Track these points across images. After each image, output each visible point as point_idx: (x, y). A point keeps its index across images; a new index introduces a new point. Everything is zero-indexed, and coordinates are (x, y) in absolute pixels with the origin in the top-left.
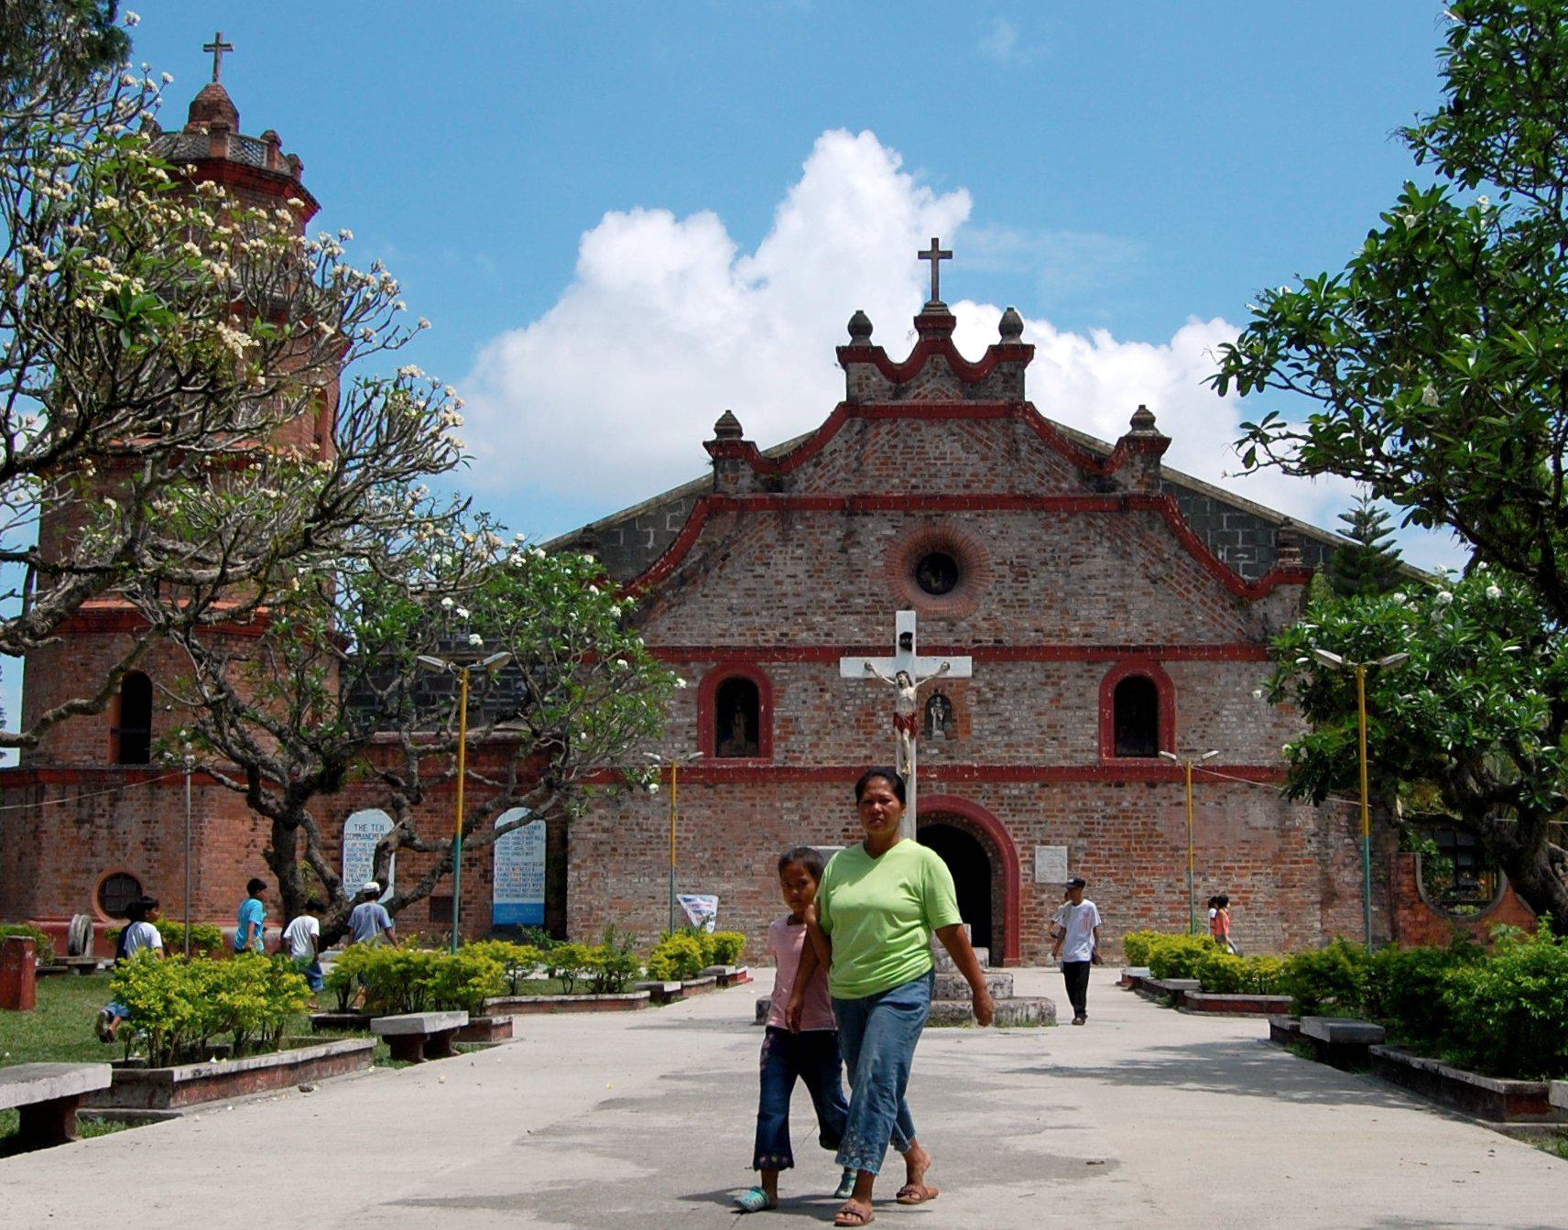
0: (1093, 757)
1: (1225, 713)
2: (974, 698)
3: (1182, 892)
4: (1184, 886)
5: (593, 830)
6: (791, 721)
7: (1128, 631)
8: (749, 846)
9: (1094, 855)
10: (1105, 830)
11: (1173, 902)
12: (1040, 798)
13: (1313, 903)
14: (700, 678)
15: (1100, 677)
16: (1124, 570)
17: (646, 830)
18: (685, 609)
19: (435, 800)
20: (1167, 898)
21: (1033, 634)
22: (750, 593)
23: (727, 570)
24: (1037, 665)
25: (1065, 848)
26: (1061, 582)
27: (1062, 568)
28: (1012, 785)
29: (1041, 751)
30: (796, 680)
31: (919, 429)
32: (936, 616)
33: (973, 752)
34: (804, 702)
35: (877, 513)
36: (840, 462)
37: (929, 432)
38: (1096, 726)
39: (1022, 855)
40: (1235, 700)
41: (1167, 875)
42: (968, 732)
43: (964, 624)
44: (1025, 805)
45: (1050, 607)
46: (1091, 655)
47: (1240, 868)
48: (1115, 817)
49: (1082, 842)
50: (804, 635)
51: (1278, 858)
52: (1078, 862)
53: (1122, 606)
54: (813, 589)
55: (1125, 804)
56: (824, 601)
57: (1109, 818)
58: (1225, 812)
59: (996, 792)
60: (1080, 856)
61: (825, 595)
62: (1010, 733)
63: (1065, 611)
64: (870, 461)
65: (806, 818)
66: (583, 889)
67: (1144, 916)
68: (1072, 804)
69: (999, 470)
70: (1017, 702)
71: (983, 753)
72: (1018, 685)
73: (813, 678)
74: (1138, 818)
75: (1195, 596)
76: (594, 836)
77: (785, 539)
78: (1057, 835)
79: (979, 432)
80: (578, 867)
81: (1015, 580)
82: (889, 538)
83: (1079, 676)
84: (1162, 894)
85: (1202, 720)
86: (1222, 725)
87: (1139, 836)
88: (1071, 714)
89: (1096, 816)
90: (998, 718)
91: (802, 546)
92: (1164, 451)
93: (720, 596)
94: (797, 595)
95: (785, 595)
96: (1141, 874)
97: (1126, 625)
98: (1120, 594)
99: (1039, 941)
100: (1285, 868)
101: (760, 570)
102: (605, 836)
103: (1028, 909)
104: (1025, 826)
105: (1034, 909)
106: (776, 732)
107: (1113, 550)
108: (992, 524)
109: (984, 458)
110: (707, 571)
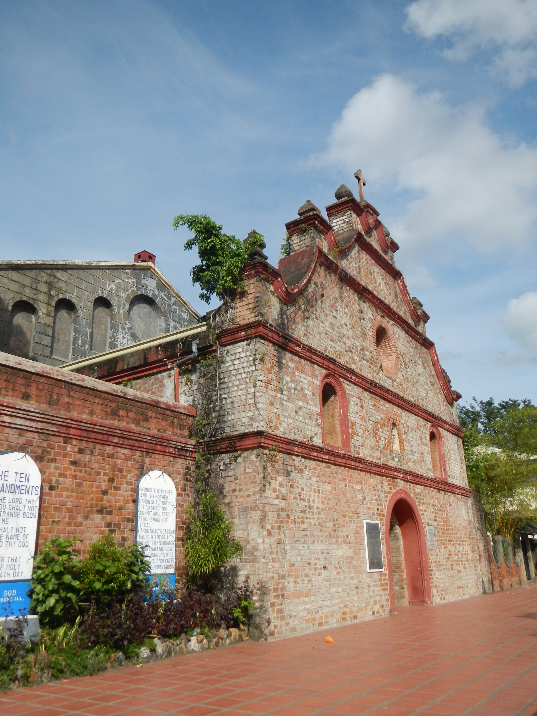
5: (277, 497)
14: (319, 378)
17: (303, 500)
18: (310, 323)
19: (81, 451)
23: (324, 306)
28: (417, 486)
32: (389, 375)
34: (357, 412)
40: (452, 452)
48: (439, 510)
49: (435, 524)
55: (441, 503)
61: (358, 344)
66: (274, 556)
67: (452, 569)
76: (276, 502)
82: (372, 320)
92: (427, 322)
95: (344, 335)
100: (472, 540)
101: (335, 313)
110: (316, 300)
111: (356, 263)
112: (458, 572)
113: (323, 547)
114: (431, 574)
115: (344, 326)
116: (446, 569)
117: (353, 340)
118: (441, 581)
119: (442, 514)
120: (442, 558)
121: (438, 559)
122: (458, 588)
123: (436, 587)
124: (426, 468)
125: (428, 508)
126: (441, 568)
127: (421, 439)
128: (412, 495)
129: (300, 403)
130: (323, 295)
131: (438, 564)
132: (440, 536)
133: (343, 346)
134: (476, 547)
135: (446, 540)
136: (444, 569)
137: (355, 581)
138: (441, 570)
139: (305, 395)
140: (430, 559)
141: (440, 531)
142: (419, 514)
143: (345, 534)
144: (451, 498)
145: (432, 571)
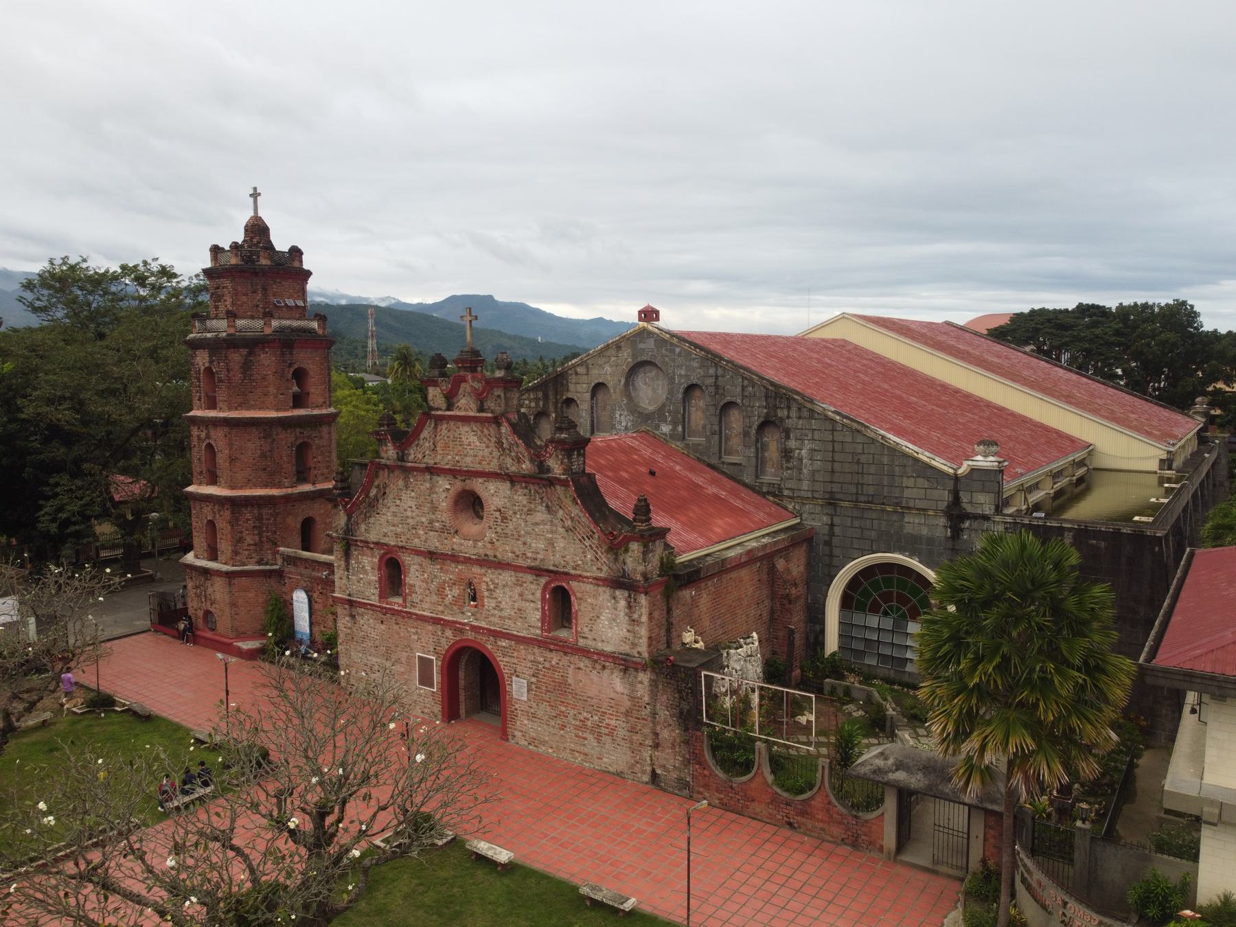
1: (603, 618)
2: (485, 587)
3: (580, 721)
4: (581, 717)
5: (345, 627)
6: (412, 586)
7: (552, 560)
8: (399, 649)
9: (539, 688)
10: (544, 676)
11: (576, 726)
12: (514, 650)
13: (647, 746)
16: (552, 522)
18: (372, 520)
21: (510, 555)
22: (394, 514)
23: (386, 501)
24: (513, 573)
25: (525, 681)
26: (523, 525)
27: (524, 517)
29: (515, 623)
30: (414, 564)
31: (458, 428)
33: (486, 618)
35: (442, 476)
36: (427, 444)
37: (464, 429)
40: (608, 611)
41: (574, 709)
42: (483, 606)
43: (480, 544)
45: (518, 540)
46: (538, 571)
47: (610, 714)
48: (549, 669)
49: (533, 680)
50: (416, 540)
51: (628, 714)
52: (532, 690)
53: (551, 543)
54: (418, 516)
55: (553, 663)
56: (423, 523)
57: (547, 668)
58: (601, 678)
59: (496, 642)
60: (533, 686)
61: (424, 520)
62: (501, 610)
63: (525, 544)
64: (439, 445)
65: (420, 639)
67: (563, 730)
69: (494, 453)
70: (504, 593)
71: (490, 619)
72: (504, 583)
73: (420, 565)
74: (559, 672)
75: (587, 543)
77: (407, 487)
78: (523, 673)
79: (486, 431)
80: (341, 644)
81: (502, 520)
83: (532, 583)
84: (571, 719)
85: (591, 620)
87: (560, 683)
88: (528, 604)
89: (540, 666)
90: (494, 601)
91: (413, 491)
93: (383, 514)
94: (413, 518)
95: (408, 517)
97: (553, 556)
98: (550, 536)
99: (516, 729)
101: (398, 502)
102: (349, 631)
103: (511, 711)
106: (407, 591)
107: (547, 506)
108: (492, 486)
109: (488, 447)
111: (429, 442)
112: (577, 736)
113: (378, 660)
115: (409, 509)
117: (418, 518)
119: (554, 674)
121: (532, 711)
122: (574, 751)
126: (534, 719)
127: (521, 595)
128: (489, 647)
129: (362, 576)
130: (385, 493)
133: (406, 526)
134: (647, 731)
139: (366, 570)
142: (499, 666)
144: (584, 663)
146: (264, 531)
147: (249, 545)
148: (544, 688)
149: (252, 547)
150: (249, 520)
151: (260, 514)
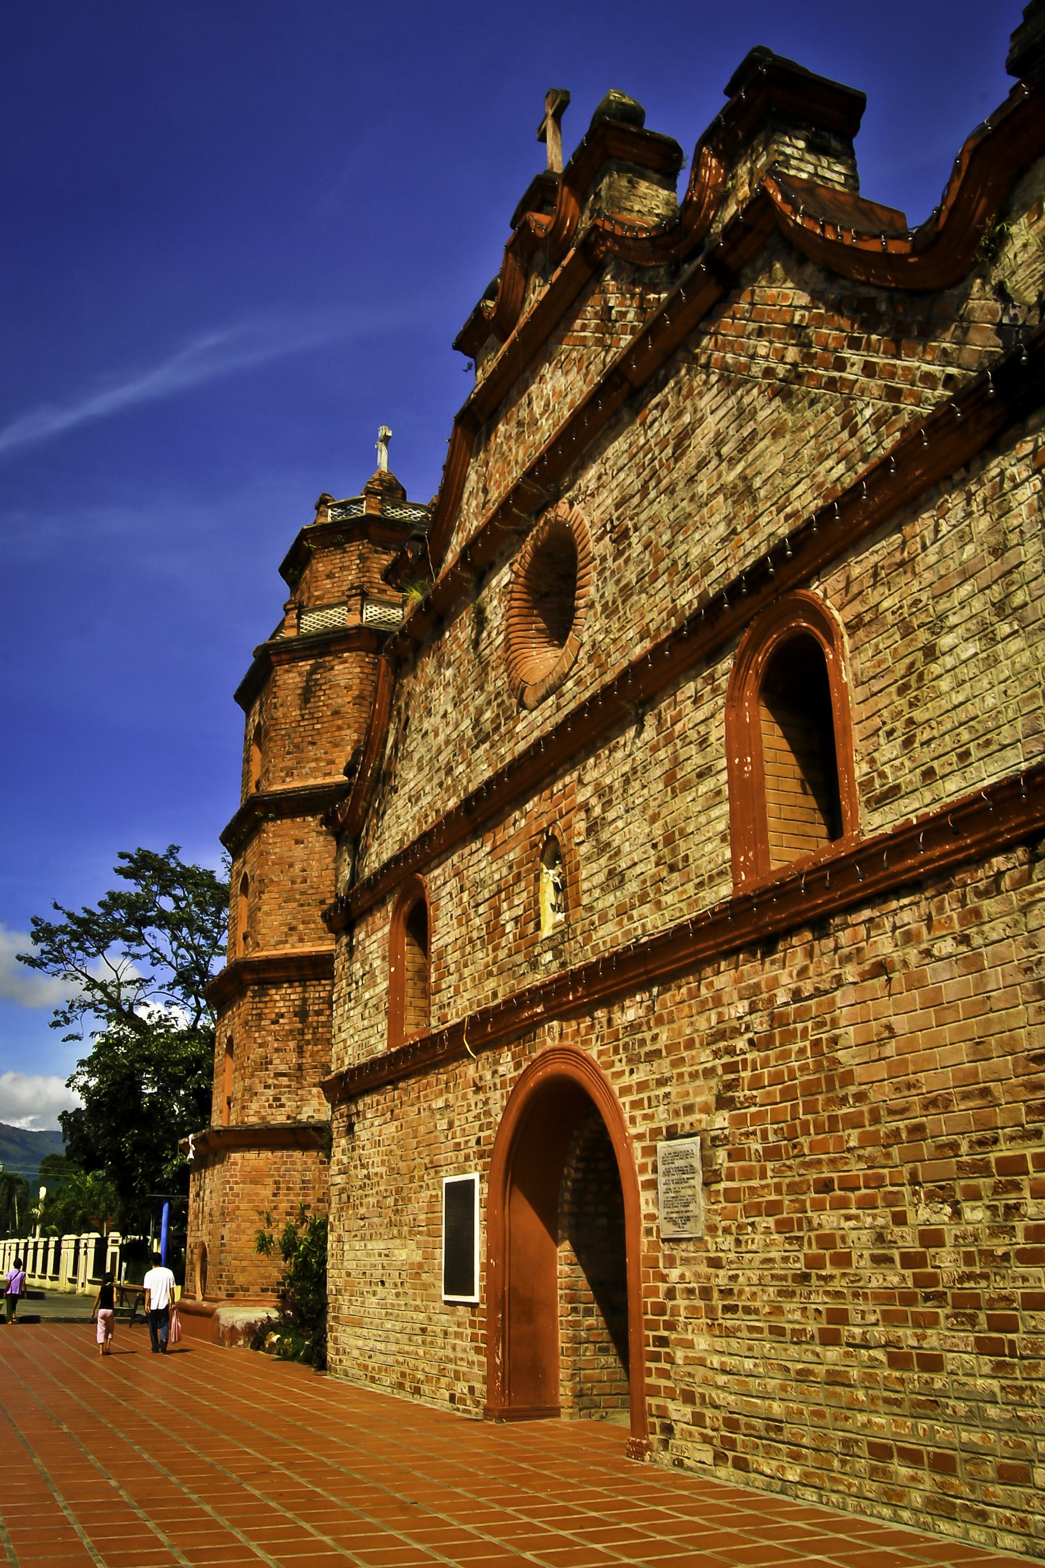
0: (725, 890)
3: (909, 1260)
4: (908, 1239)
15: (723, 682)
20: (877, 1280)
38: (726, 807)
39: (643, 1168)
41: (868, 1204)
43: (570, 684)
44: (643, 1042)
49: (721, 1120)
55: (782, 997)
60: (721, 1155)
68: (702, 1023)
86: (945, 685)
89: (741, 1043)
96: (819, 1206)
104: (644, 1095)
105: (660, 1309)
112: (899, 1360)
114: (663, 1341)
116: (777, 1331)
118: (721, 1379)
120: (749, 1275)
121: (722, 1278)
123: (688, 1397)
124: (690, 887)
125: (674, 1064)
131: (718, 1303)
132: (747, 1174)
135: (794, 1189)
136: (752, 1329)
137: (422, 1316)
138: (730, 1333)
140: (664, 1278)
141: (756, 1145)
143: (411, 1217)
145: (671, 1326)
146: (308, 1043)
147: (278, 1075)
148: (756, 1145)
149: (284, 1081)
150: (282, 1016)
151: (304, 1000)
